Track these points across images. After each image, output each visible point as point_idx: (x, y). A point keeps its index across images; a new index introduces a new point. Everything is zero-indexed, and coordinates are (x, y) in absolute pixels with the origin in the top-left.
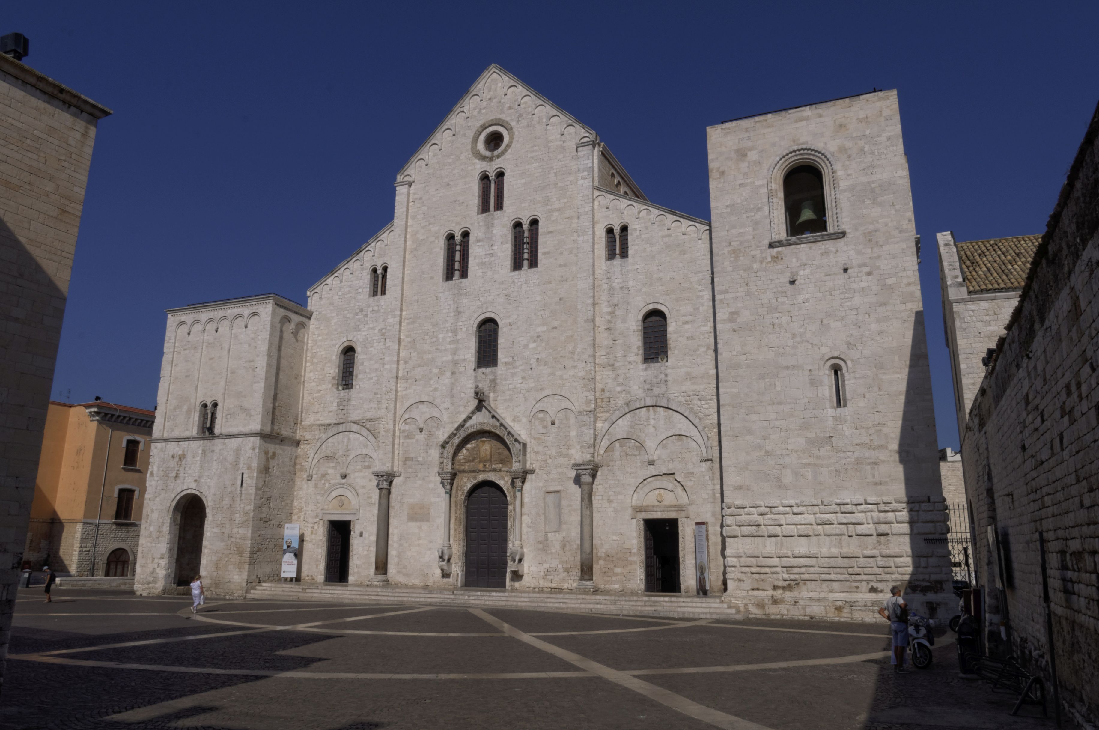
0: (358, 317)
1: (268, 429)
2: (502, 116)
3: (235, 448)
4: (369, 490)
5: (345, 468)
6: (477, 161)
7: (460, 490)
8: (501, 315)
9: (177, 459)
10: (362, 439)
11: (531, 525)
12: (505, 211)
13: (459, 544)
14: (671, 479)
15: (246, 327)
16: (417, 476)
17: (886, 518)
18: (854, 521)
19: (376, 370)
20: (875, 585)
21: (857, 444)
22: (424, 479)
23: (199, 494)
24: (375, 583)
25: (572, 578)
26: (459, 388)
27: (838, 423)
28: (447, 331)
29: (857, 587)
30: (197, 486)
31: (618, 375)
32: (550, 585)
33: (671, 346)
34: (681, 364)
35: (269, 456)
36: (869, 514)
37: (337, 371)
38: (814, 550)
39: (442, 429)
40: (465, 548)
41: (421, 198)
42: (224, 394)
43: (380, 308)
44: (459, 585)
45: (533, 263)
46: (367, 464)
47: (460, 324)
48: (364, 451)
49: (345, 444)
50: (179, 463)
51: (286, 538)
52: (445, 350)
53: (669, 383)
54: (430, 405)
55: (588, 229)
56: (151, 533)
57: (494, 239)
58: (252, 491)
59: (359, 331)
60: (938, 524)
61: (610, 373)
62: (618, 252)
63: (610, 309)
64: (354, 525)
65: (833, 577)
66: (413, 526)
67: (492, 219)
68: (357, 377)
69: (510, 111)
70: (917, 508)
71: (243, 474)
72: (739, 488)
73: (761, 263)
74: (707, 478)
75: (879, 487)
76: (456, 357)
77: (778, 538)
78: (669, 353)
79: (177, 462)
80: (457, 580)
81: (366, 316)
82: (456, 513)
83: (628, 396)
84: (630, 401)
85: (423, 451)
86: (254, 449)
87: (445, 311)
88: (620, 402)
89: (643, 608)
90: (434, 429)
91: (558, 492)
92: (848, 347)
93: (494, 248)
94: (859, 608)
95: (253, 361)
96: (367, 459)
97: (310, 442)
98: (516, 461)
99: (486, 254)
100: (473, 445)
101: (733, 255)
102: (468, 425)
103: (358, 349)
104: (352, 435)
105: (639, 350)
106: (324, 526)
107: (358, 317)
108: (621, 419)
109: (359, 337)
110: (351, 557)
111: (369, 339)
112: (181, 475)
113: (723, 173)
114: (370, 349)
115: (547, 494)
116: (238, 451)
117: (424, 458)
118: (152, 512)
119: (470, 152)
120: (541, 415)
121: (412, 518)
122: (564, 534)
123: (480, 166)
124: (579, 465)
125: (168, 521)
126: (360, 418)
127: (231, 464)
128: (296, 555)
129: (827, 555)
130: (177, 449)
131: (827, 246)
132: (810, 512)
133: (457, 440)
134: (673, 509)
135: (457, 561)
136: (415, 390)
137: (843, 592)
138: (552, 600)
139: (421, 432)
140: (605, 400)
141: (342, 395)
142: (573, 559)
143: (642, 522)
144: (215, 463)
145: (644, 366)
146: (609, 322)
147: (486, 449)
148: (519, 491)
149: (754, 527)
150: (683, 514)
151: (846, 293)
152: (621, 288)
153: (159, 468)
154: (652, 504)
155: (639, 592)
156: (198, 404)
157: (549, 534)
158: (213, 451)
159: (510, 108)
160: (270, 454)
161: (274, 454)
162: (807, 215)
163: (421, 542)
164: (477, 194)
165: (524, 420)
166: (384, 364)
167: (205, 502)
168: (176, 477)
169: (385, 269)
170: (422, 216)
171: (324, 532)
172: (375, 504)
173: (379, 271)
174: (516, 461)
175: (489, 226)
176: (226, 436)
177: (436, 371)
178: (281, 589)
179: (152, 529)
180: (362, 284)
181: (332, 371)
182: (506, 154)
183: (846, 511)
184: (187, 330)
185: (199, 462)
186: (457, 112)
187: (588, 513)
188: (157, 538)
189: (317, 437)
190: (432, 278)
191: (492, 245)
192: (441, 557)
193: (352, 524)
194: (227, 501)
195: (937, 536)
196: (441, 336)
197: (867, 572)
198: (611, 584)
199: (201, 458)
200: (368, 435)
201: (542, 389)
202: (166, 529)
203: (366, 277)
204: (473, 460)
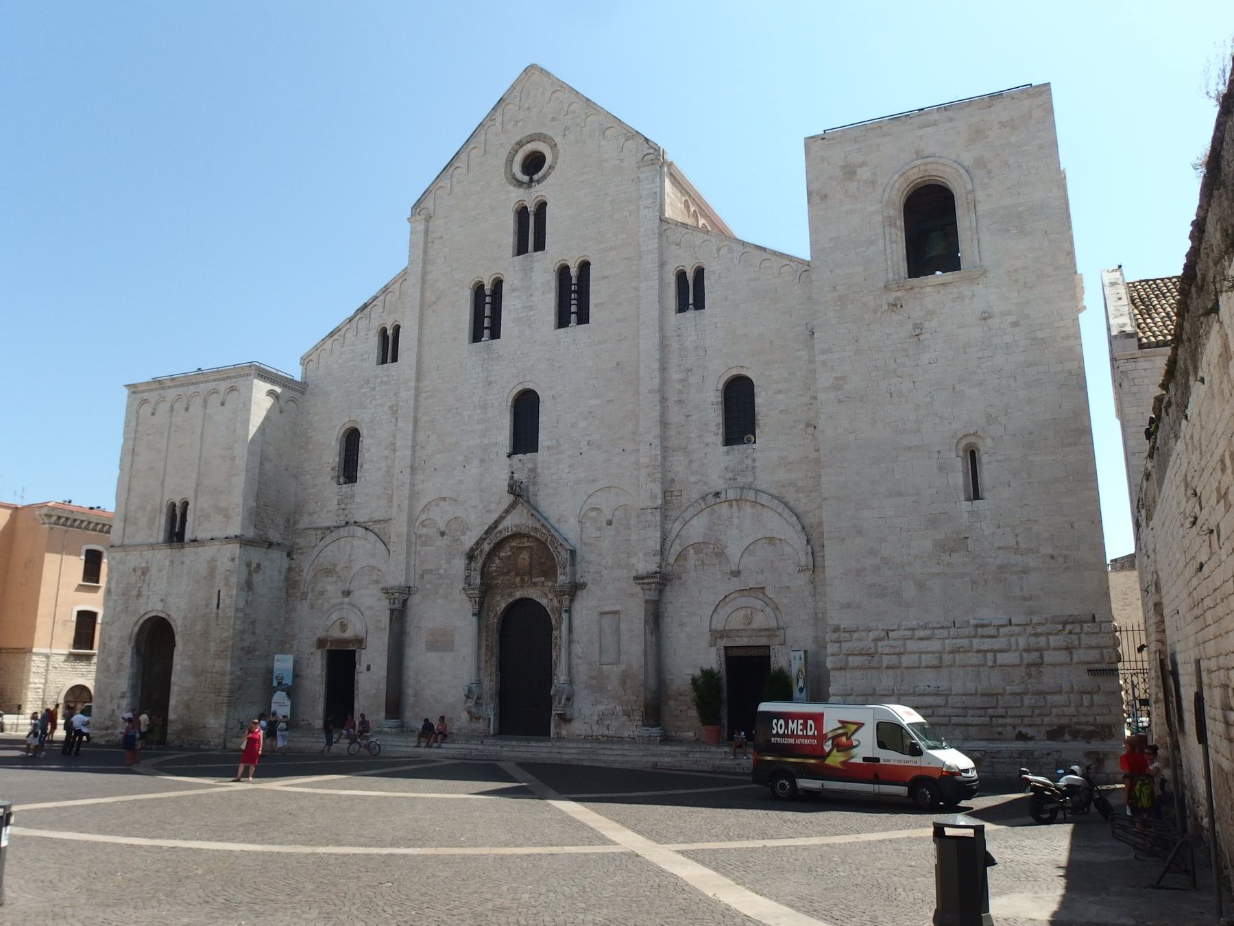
1: (251, 533)
2: (544, 130)
5: (348, 584)
6: (511, 188)
7: (492, 611)
9: (139, 573)
11: (582, 655)
13: (491, 681)
14: (761, 596)
15: (223, 404)
16: (437, 593)
17: (1038, 643)
18: (996, 647)
19: (387, 457)
20: (1024, 730)
21: (999, 548)
24: (386, 729)
25: (635, 723)
26: (489, 480)
27: (975, 520)
28: (474, 406)
29: (1000, 733)
30: (163, 606)
31: (691, 461)
33: (761, 422)
34: (773, 445)
35: (252, 568)
36: (1013, 639)
37: (337, 460)
38: (944, 685)
39: (468, 533)
40: (498, 686)
41: (441, 238)
42: (196, 491)
44: (492, 731)
45: (583, 318)
46: (374, 578)
47: (491, 397)
48: (372, 562)
50: (142, 578)
51: (276, 674)
55: (653, 272)
56: (108, 666)
57: (533, 287)
58: (231, 612)
60: (1105, 651)
61: (683, 458)
62: (691, 301)
63: (680, 376)
64: (360, 656)
65: (969, 720)
66: (433, 657)
68: (362, 467)
69: (553, 123)
70: (1077, 630)
71: (219, 591)
72: (848, 606)
73: (875, 313)
74: (807, 593)
75: (1027, 603)
76: (486, 441)
77: (898, 671)
78: (757, 431)
80: (489, 727)
81: (374, 389)
82: (487, 641)
83: (705, 487)
84: (707, 495)
87: (471, 381)
88: (695, 496)
89: (723, 762)
90: (459, 533)
91: (616, 612)
92: (988, 421)
93: (533, 299)
94: (1002, 760)
95: (231, 448)
97: (304, 550)
98: (561, 574)
99: (523, 307)
100: (508, 553)
101: (838, 303)
102: (501, 527)
103: (364, 432)
105: (718, 429)
106: (322, 658)
108: (695, 518)
112: (145, 592)
113: (826, 196)
115: (602, 616)
117: (445, 570)
119: (503, 177)
120: (594, 514)
121: (433, 646)
122: (623, 667)
123: (516, 196)
124: (643, 578)
125: (129, 651)
126: (366, 519)
128: (289, 695)
129: (961, 692)
131: (961, 289)
132: (939, 636)
133: (487, 547)
134: (763, 633)
135: (488, 702)
137: (982, 740)
138: (606, 752)
140: (675, 494)
141: (344, 490)
142: (635, 698)
143: (722, 652)
146: (681, 392)
147: (524, 559)
148: (566, 611)
149: (866, 657)
150: (777, 640)
151: (985, 350)
152: (696, 348)
154: (736, 628)
156: (164, 503)
159: (553, 119)
160: (254, 566)
161: (259, 566)
162: (937, 248)
164: (512, 230)
165: (573, 520)
166: (395, 451)
167: (174, 627)
169: (397, 329)
170: (443, 260)
171: (322, 665)
172: (385, 629)
173: (390, 332)
174: (561, 574)
175: (527, 271)
177: (461, 458)
181: (331, 461)
182: (548, 178)
183: (984, 634)
184: (150, 410)
185: (165, 577)
186: (487, 126)
187: (654, 639)
188: (117, 672)
189: (313, 545)
190: (455, 339)
191: (531, 295)
192: (468, 697)
195: (1104, 666)
196: (466, 413)
197: (1013, 714)
198: (683, 731)
201: (594, 480)
202: (127, 660)
203: (374, 342)
204: (509, 572)
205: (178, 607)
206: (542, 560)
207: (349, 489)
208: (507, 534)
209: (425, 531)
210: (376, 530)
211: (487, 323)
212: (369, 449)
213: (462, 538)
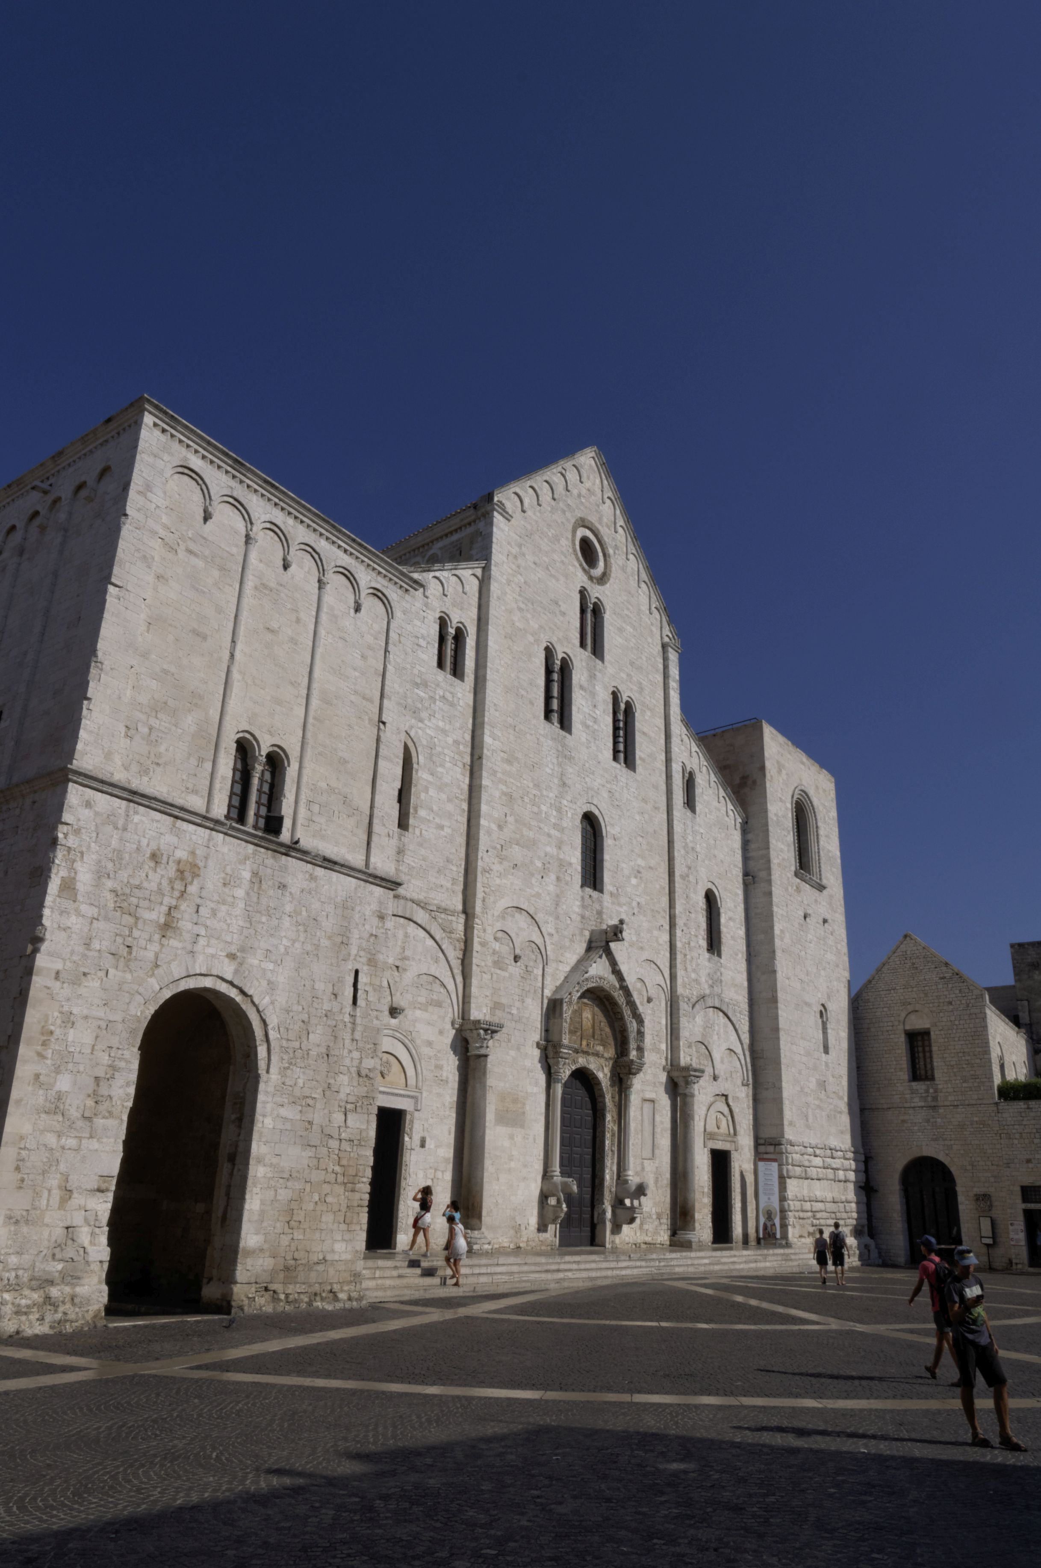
3: (339, 899)
4: (439, 1052)
8: (606, 819)
10: (430, 942)
12: (606, 668)
16: (509, 1041)
22: (518, 1049)
23: (238, 998)
46: (435, 997)
49: (399, 943)
52: (549, 835)
53: (723, 984)
54: (529, 920)
59: (421, 721)
64: (412, 1122)
67: (595, 667)
79: (171, 881)
80: (555, 1236)
81: (433, 699)
85: (517, 998)
86: (382, 917)
90: (531, 964)
96: (437, 987)
104: (411, 928)
109: (420, 732)
110: (402, 1191)
111: (439, 749)
114: (440, 769)
116: (346, 907)
117: (518, 1009)
118: (68, 1020)
121: (503, 1119)
127: (330, 938)
130: (169, 839)
136: (512, 884)
139: (516, 962)
144: (287, 922)
145: (707, 955)
147: (587, 1018)
153: (100, 874)
158: (283, 887)
163: (513, 1164)
168: (167, 927)
176: (325, 859)
179: (64, 1083)
180: (424, 632)
193: (408, 1117)
194: (318, 1036)
196: (544, 808)
199: (248, 894)
200: (442, 939)
204: (576, 1032)
205: (270, 982)
209: (497, 946)
210: (440, 921)
211: (555, 705)
212: (426, 790)
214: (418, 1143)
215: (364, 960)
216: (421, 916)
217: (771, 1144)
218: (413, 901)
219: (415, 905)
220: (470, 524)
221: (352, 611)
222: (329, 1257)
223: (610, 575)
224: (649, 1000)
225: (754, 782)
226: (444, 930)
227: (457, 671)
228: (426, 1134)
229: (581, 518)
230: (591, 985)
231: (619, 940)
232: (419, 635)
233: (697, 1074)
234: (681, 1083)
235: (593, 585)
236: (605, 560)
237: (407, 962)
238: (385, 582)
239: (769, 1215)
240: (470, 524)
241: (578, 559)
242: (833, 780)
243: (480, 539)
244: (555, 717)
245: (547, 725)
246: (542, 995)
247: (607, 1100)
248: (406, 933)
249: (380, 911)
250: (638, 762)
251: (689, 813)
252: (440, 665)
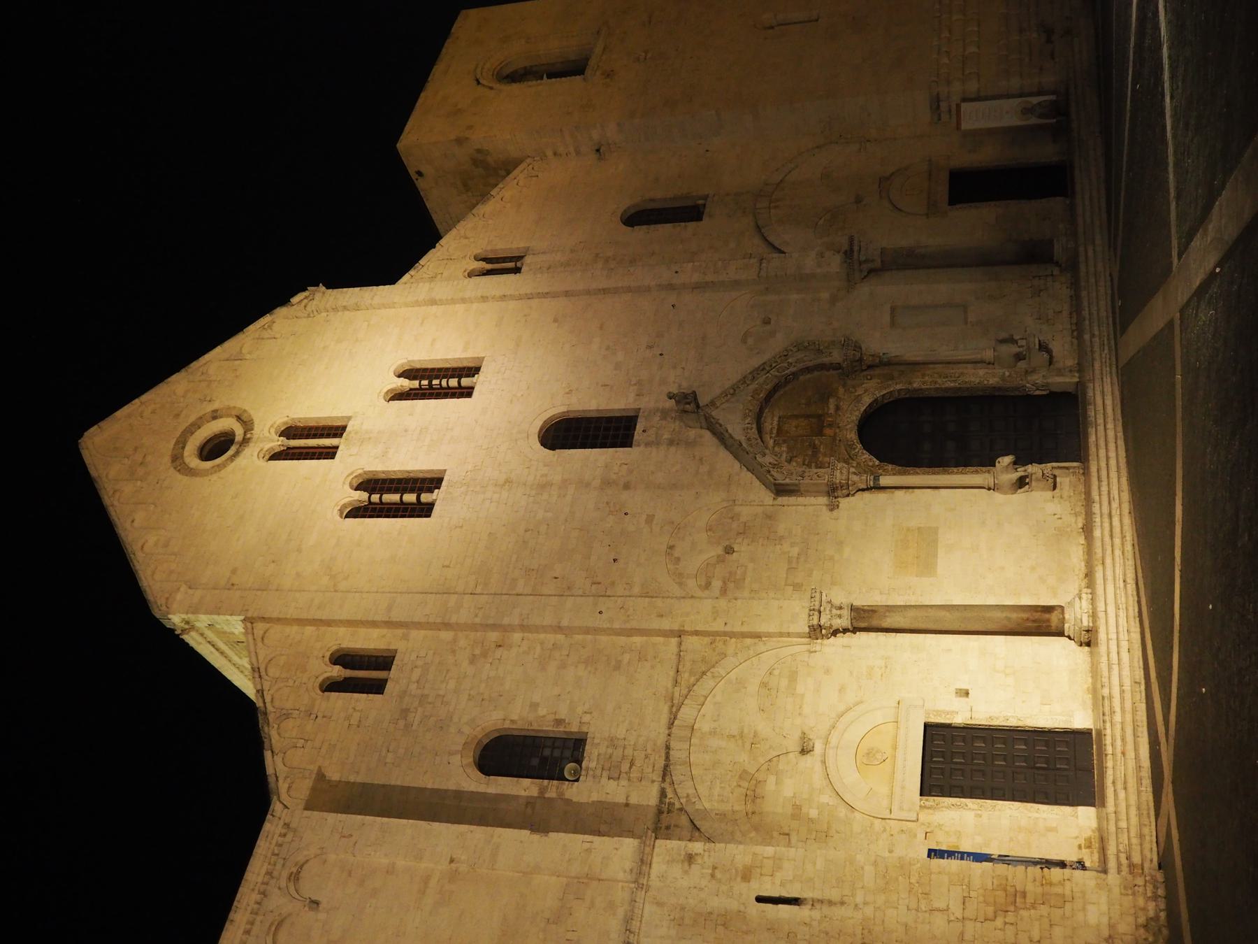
0: (416, 723)
32: (1065, 313)
43: (420, 663)
46: (784, 682)
48: (753, 687)
64: (938, 713)
67: (356, 433)
68: (559, 722)
80: (1067, 468)
81: (423, 699)
86: (690, 858)
90: (734, 525)
100: (784, 449)
104: (704, 726)
107: (416, 723)
117: (793, 544)
119: (210, 477)
139: (734, 551)
141: (593, 765)
145: (705, 218)
147: (796, 427)
155: (1068, 202)
157: (969, 320)
178: (1122, 794)
200: (713, 677)
206: (803, 401)
207: (595, 756)
208: (755, 430)
209: (716, 584)
210: (692, 679)
211: (410, 498)
212: (534, 706)
213: (743, 519)
214: (964, 699)
215: (744, 885)
216: (686, 713)
217: (938, 107)
218: (671, 724)
219: (676, 722)
220: (202, 635)
221: (322, 916)
222: (1106, 933)
223: (240, 409)
224: (767, 322)
225: (479, 151)
226: (704, 673)
227: (384, 661)
228: (953, 689)
229: (173, 461)
230: (754, 432)
231: (695, 399)
232: (346, 723)
233: (856, 248)
234: (865, 267)
235: (255, 437)
236: (221, 417)
237: (746, 731)
238: (279, 866)
239: (1027, 111)
240: (202, 635)
241: (224, 465)
242: (464, 12)
243: (218, 626)
244: (425, 498)
245: (436, 510)
246: (773, 505)
247: (898, 387)
248: (710, 733)
249: (683, 861)
250: (470, 354)
251: (528, 260)
252: (377, 687)
